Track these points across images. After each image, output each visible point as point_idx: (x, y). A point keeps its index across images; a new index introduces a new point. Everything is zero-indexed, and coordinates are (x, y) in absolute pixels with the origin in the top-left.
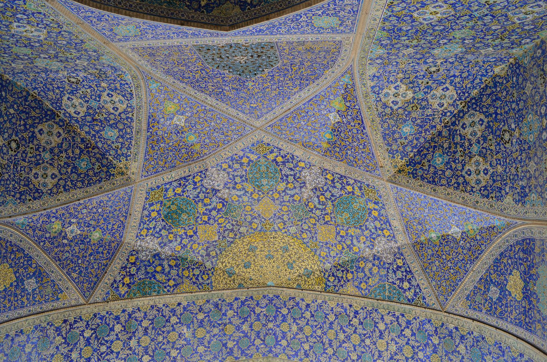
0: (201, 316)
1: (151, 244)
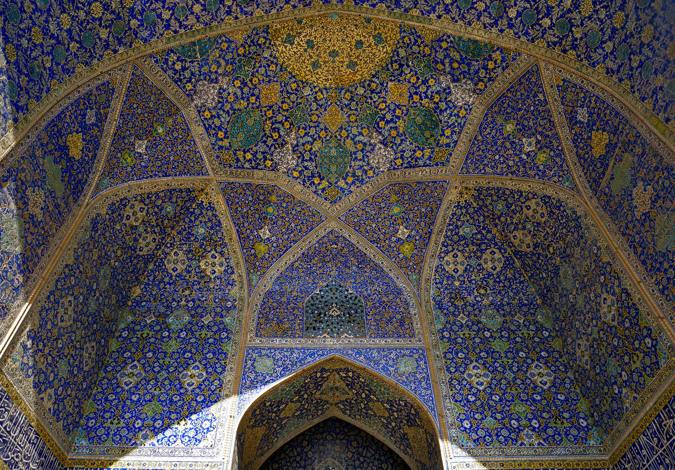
1: (460, 95)
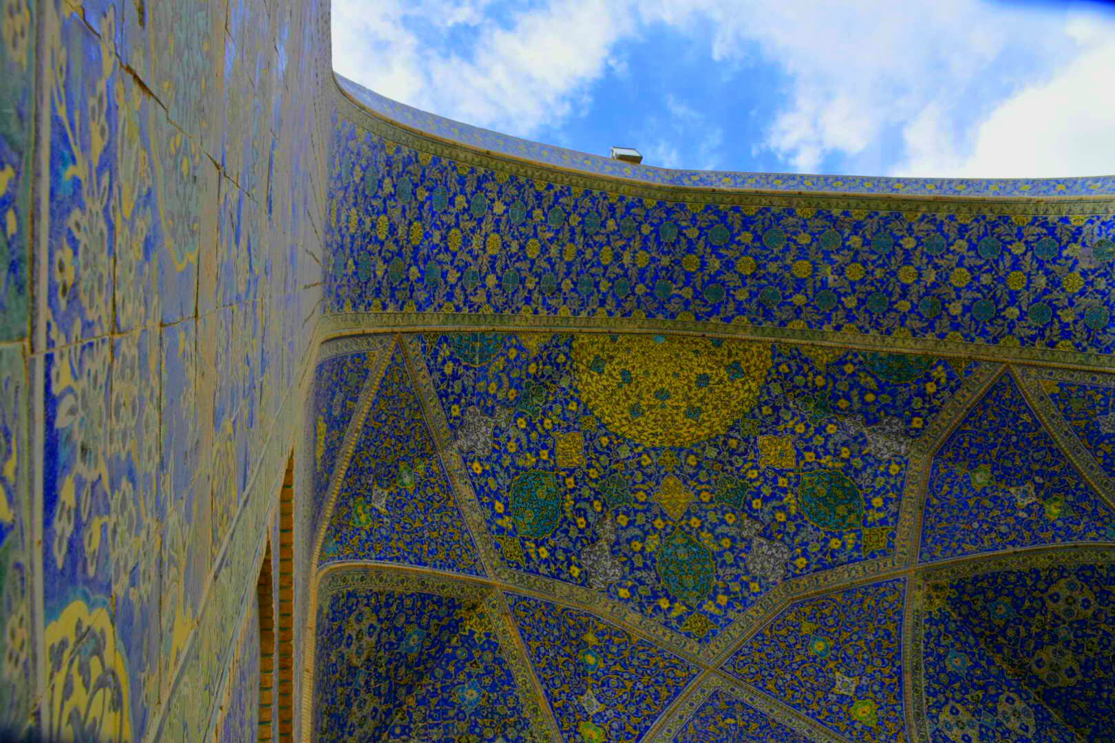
0: (799, 299)
1: (881, 444)
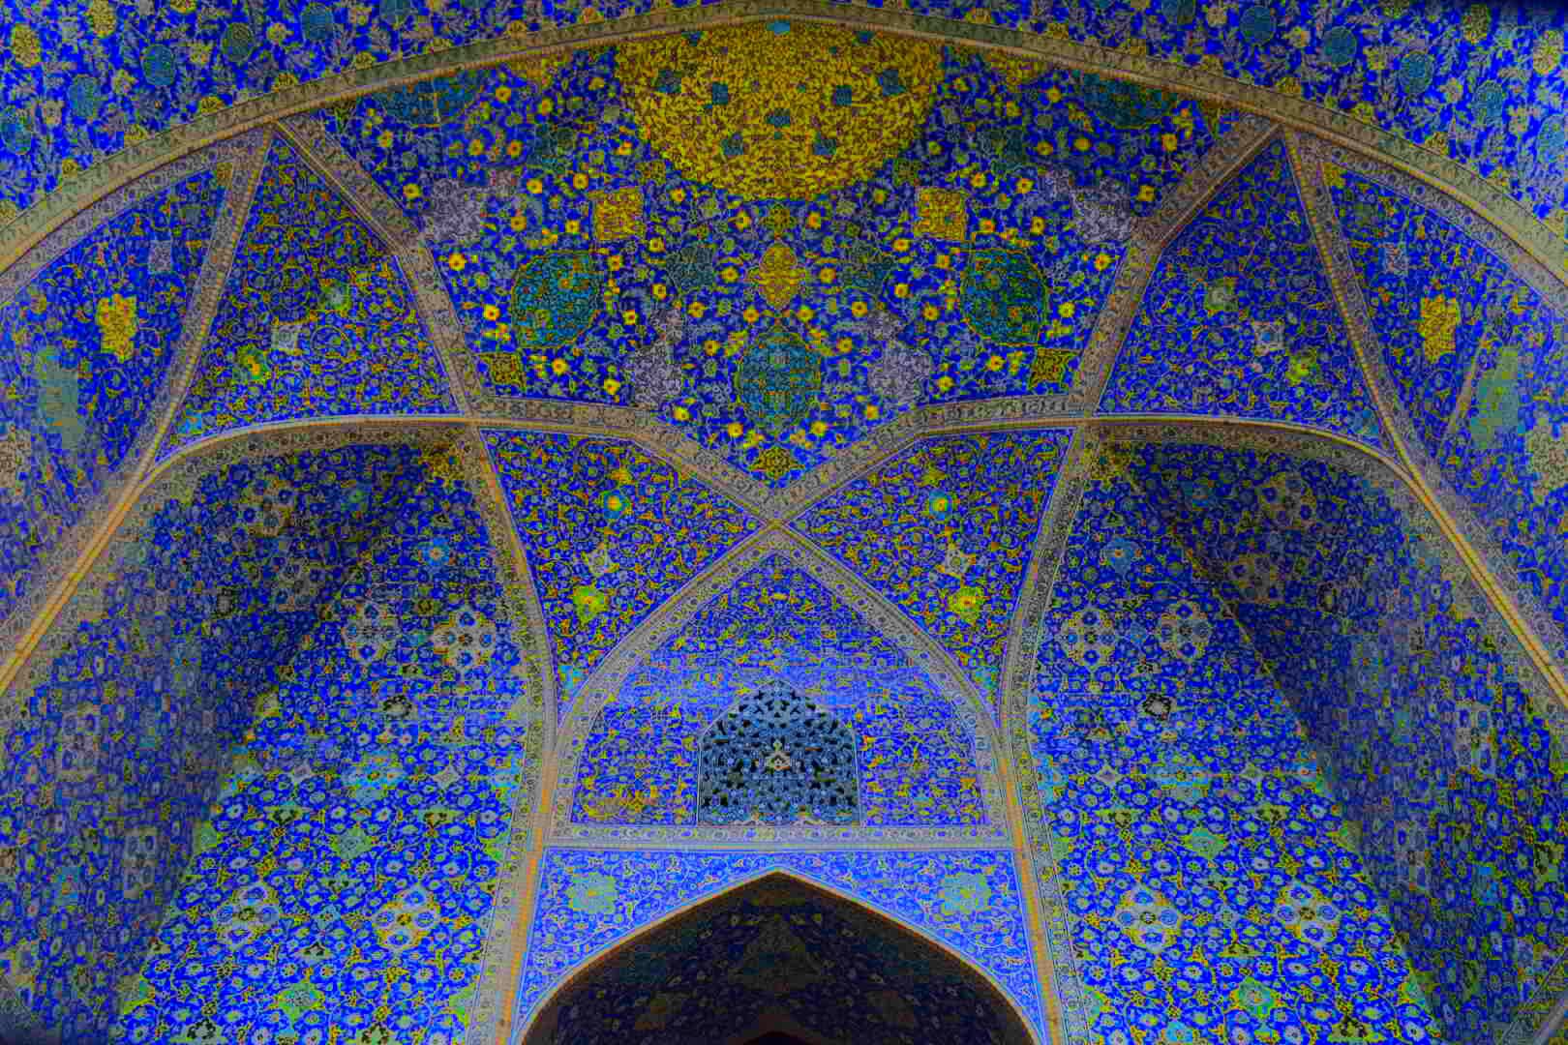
1: (1092, 218)
